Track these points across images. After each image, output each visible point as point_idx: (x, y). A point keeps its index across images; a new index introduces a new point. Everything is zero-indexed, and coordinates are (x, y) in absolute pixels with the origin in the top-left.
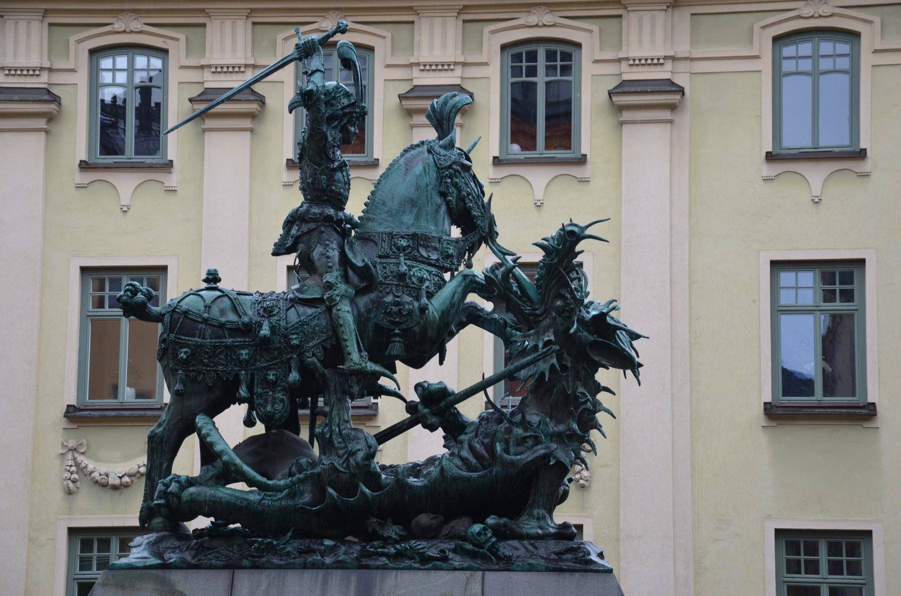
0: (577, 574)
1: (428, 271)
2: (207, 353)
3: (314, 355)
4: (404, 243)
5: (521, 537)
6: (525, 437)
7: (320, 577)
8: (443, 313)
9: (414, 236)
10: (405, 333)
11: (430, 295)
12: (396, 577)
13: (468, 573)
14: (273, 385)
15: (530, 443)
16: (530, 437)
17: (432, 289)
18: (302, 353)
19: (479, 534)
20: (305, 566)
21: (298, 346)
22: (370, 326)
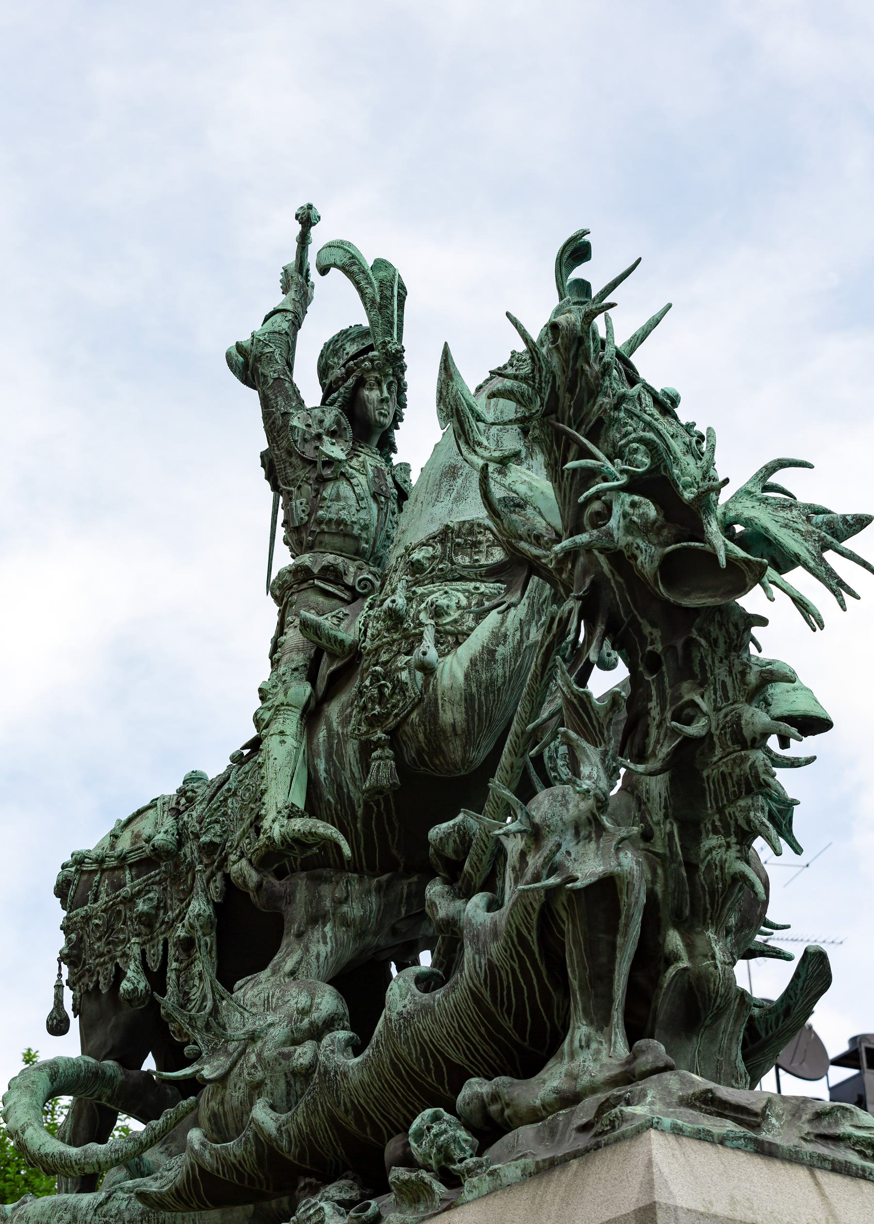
0: (574, 1163)
1: (464, 591)
4: (417, 555)
5: (534, 1116)
8: (473, 662)
9: (445, 535)
10: (395, 738)
11: (451, 638)
17: (469, 621)
19: (419, 1135)
21: (210, 849)
22: (351, 749)
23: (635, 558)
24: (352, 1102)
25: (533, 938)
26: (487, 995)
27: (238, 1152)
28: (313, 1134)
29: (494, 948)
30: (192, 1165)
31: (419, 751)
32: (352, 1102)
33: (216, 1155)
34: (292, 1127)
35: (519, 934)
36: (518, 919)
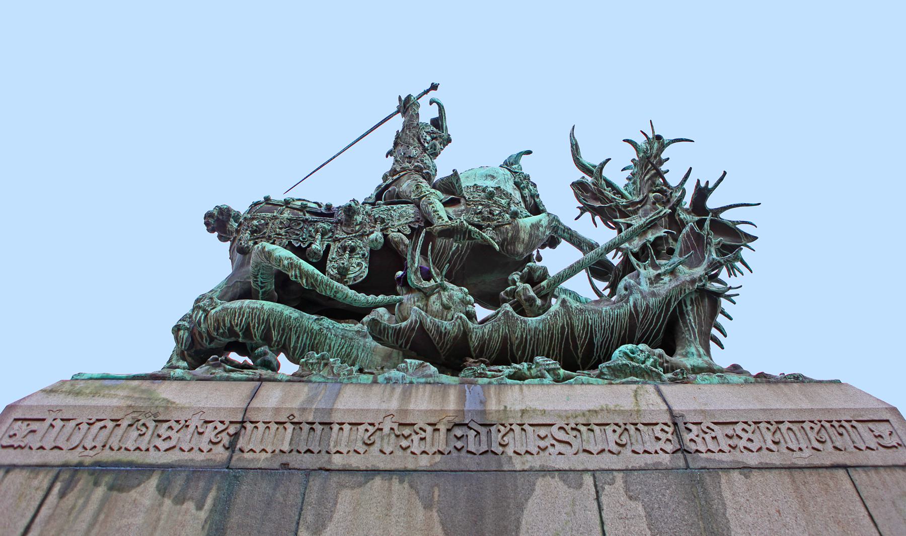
2: (281, 223)
3: (399, 231)
6: (659, 275)
7: (399, 390)
12: (521, 389)
13: (634, 387)
14: (353, 250)
15: (666, 279)
16: (665, 274)
18: (386, 229)
20: (375, 382)
23: (679, 215)
24: (522, 335)
25: (674, 304)
26: (641, 317)
27: (449, 328)
28: (489, 341)
29: (652, 301)
30: (416, 322)
31: (504, 240)
32: (522, 335)
33: (434, 324)
34: (480, 332)
35: (670, 300)
36: (674, 293)
